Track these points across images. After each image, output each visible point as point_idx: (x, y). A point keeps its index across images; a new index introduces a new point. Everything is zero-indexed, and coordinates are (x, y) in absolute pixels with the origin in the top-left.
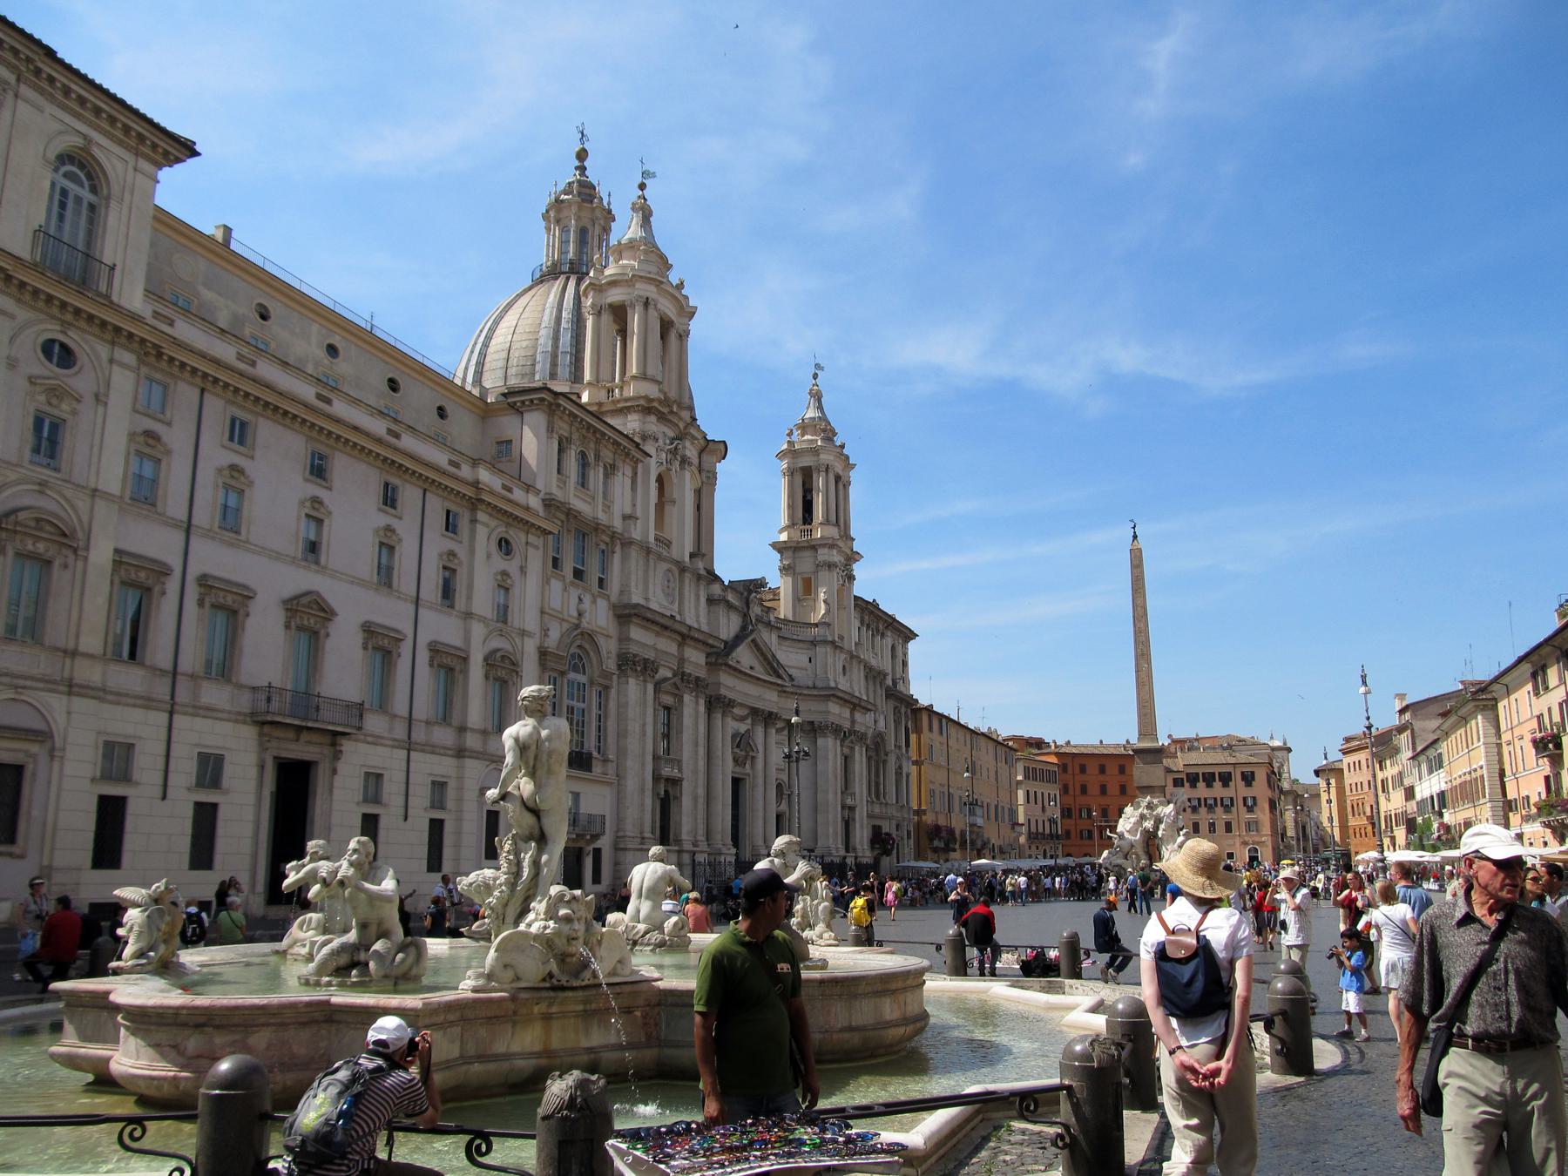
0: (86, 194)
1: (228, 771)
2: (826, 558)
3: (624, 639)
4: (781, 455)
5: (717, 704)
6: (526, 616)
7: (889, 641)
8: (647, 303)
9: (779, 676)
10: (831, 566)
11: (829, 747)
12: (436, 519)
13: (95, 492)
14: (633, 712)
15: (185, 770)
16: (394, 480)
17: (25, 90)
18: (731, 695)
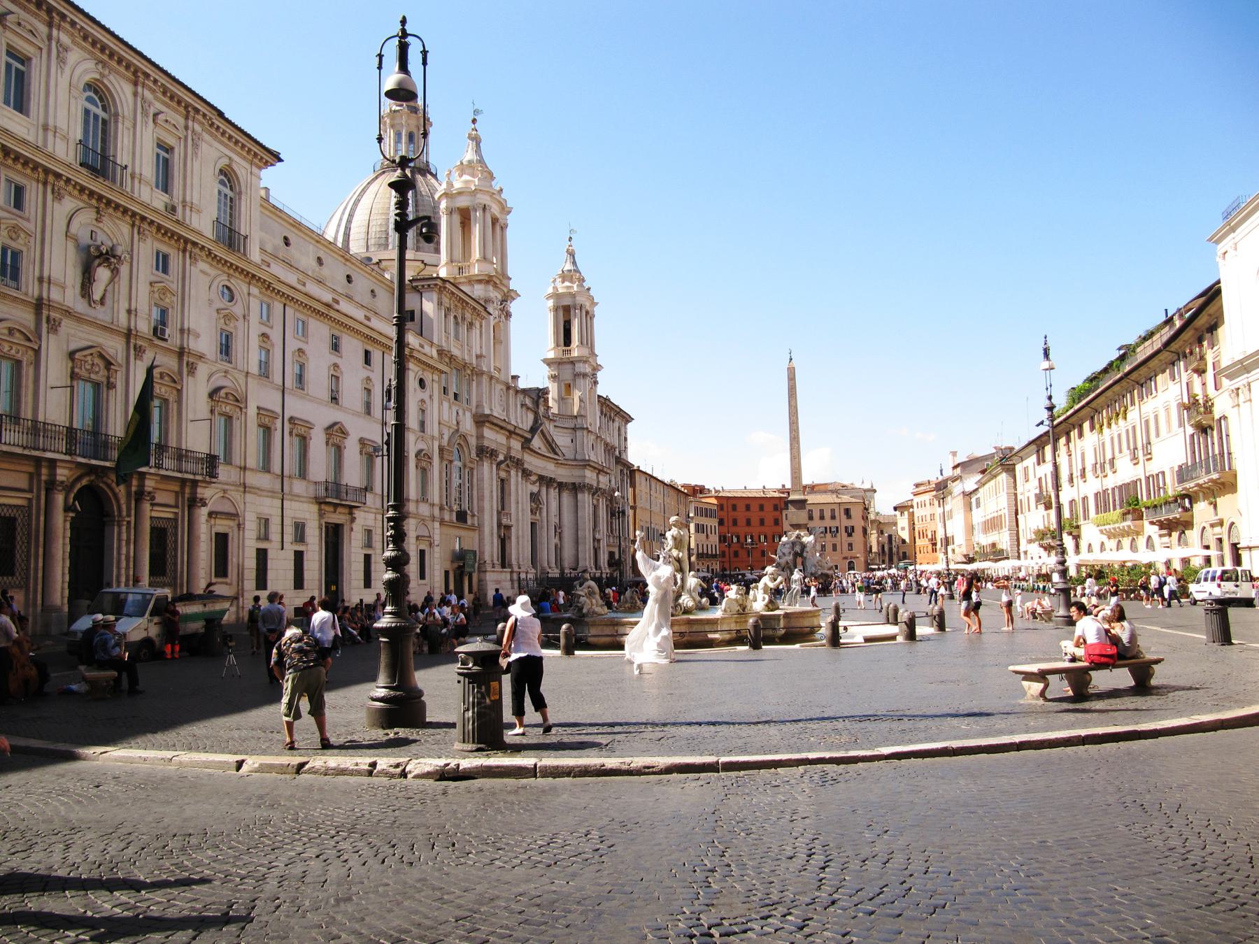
0: (227, 191)
2: (582, 370)
3: (480, 437)
5: (526, 474)
6: (433, 428)
7: (616, 424)
8: (484, 208)
9: (556, 453)
10: (585, 375)
11: (585, 499)
14: (486, 485)
16: (369, 348)
17: (206, 137)
18: (530, 468)
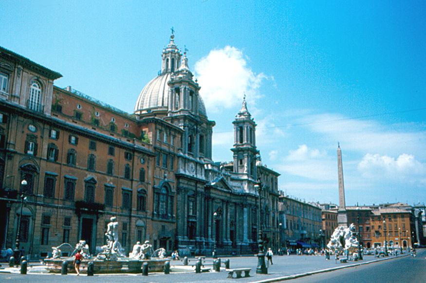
1: (72, 222)
3: (178, 183)
4: (234, 123)
12: (123, 155)
13: (41, 159)
15: (61, 222)
